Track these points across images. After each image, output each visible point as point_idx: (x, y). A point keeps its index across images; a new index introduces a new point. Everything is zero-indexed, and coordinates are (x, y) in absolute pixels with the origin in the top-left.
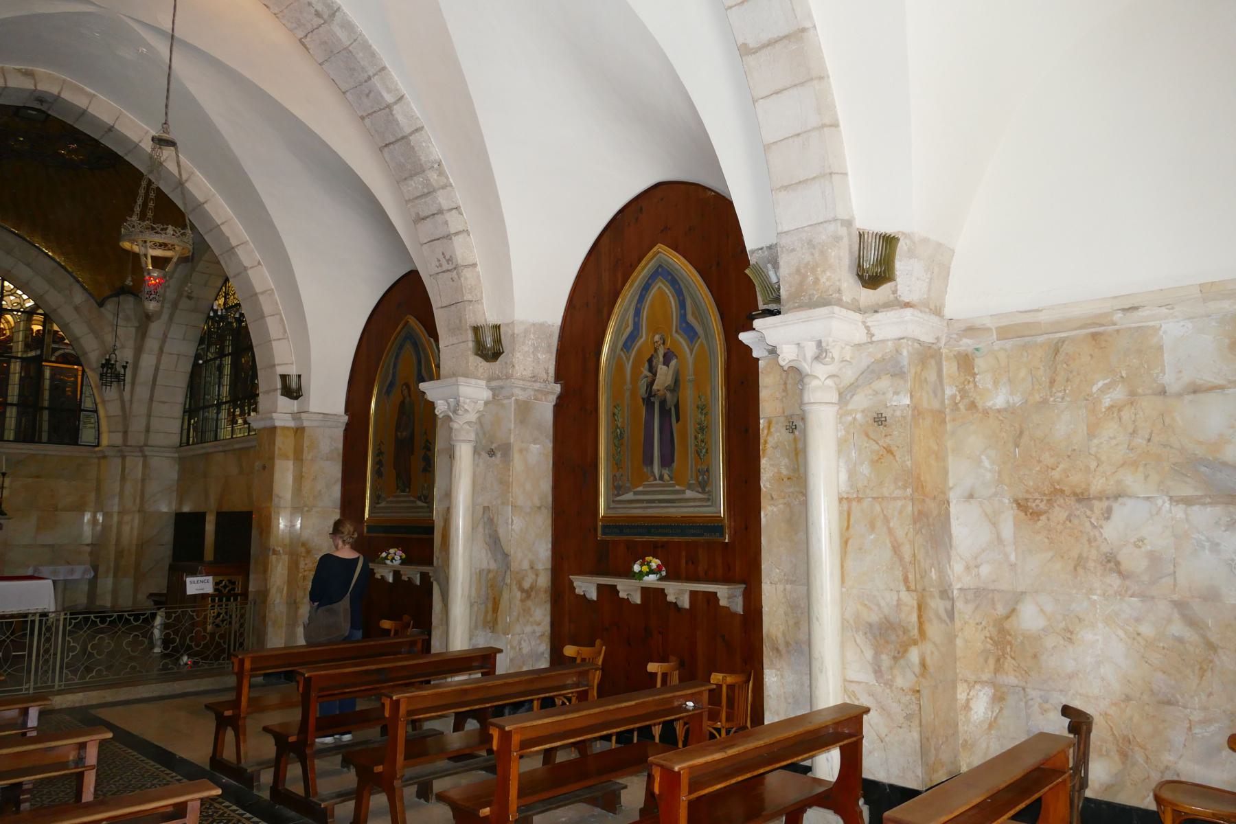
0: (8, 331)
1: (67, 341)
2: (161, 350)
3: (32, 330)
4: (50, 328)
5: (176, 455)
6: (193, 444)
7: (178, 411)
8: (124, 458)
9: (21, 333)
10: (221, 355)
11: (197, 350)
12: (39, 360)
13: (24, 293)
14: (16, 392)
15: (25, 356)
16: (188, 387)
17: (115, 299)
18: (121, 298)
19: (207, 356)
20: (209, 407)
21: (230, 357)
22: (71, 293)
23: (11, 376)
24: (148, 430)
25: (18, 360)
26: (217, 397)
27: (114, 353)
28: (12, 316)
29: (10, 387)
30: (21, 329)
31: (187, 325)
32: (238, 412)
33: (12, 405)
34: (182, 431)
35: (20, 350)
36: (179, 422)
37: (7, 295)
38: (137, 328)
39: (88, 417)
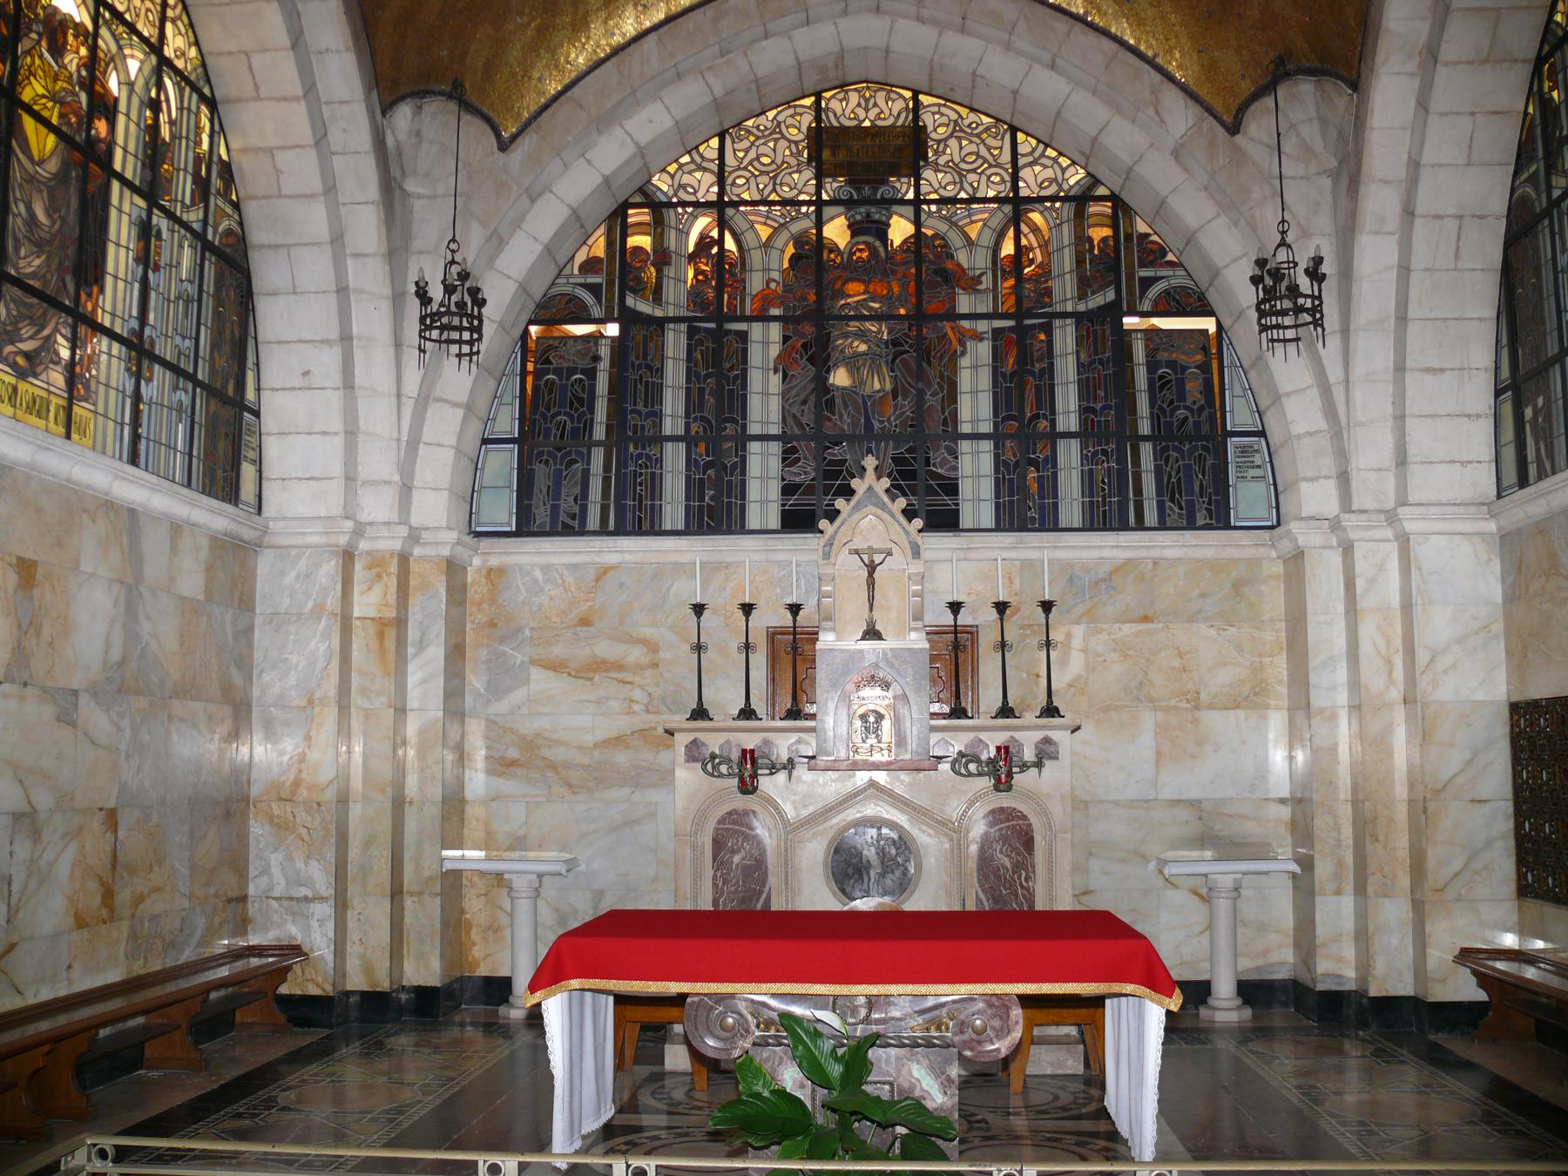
0: (1038, 252)
1: (1170, 257)
2: (1409, 213)
3: (1090, 240)
4: (1129, 230)
5: (1492, 526)
6: (1541, 475)
8: (1347, 549)
9: (1066, 251)
11: (1513, 190)
12: (1114, 312)
13: (1061, 154)
14: (1073, 404)
15: (1081, 308)
16: (1499, 314)
17: (1268, 102)
18: (1282, 91)
22: (1157, 112)
23: (1058, 363)
24: (1402, 461)
25: (1069, 321)
28: (1041, 213)
29: (1058, 391)
30: (1066, 242)
31: (1473, 114)
33: (1068, 435)
34: (1497, 453)
35: (1069, 296)
36: (1487, 425)
37: (1025, 166)
38: (1335, 175)
39: (1244, 451)
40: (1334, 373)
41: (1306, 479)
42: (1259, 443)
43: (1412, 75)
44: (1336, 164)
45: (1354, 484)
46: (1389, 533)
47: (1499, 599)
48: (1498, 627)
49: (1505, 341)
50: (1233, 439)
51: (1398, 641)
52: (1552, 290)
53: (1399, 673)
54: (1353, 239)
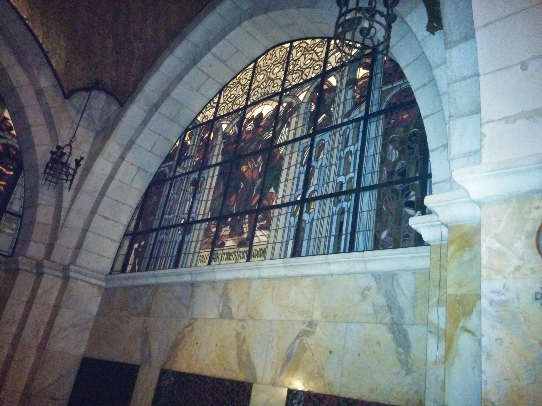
2: (122, 158)
5: (103, 284)
6: (133, 270)
7: (118, 232)
8: (40, 275)
10: (203, 166)
11: (160, 167)
16: (137, 207)
17: (85, 94)
18: (94, 93)
19: (175, 171)
20: (168, 227)
21: (218, 168)
26: (186, 216)
27: (71, 146)
31: (160, 135)
32: (226, 231)
39: (10, 221)
40: (66, 204)
41: (34, 241)
42: (18, 221)
43: (145, 111)
44: (100, 129)
45: (55, 250)
46: (61, 275)
47: (95, 314)
48: (91, 324)
49: (136, 218)
50: (8, 215)
51: (46, 320)
52: (163, 206)
53: (41, 334)
54: (97, 158)
